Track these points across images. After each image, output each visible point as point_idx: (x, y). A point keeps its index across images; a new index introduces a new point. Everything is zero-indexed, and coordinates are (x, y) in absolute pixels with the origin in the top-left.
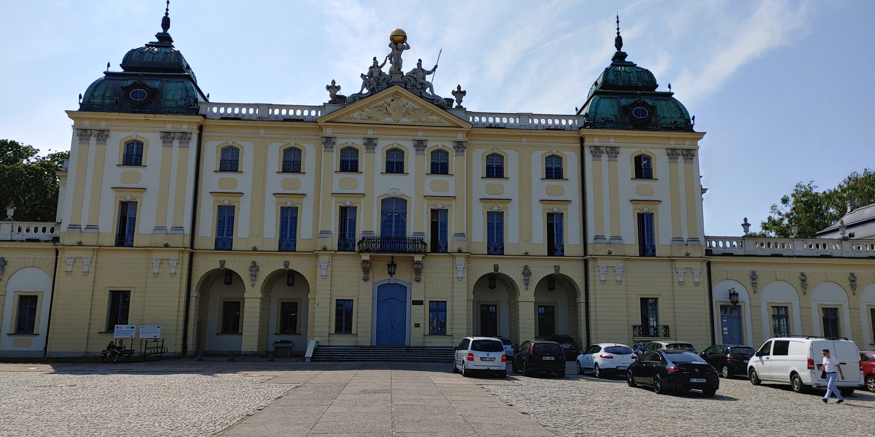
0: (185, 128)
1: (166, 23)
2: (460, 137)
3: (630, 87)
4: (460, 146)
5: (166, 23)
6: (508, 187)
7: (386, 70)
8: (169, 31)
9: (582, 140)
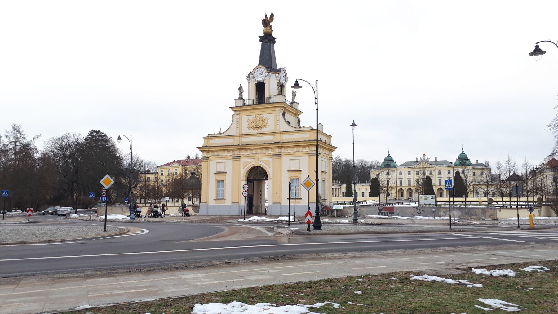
0: (394, 170)
1: (389, 152)
2: (434, 169)
3: (463, 158)
4: (434, 170)
5: (389, 152)
6: (442, 176)
7: (422, 159)
8: (389, 154)
9: (453, 168)
